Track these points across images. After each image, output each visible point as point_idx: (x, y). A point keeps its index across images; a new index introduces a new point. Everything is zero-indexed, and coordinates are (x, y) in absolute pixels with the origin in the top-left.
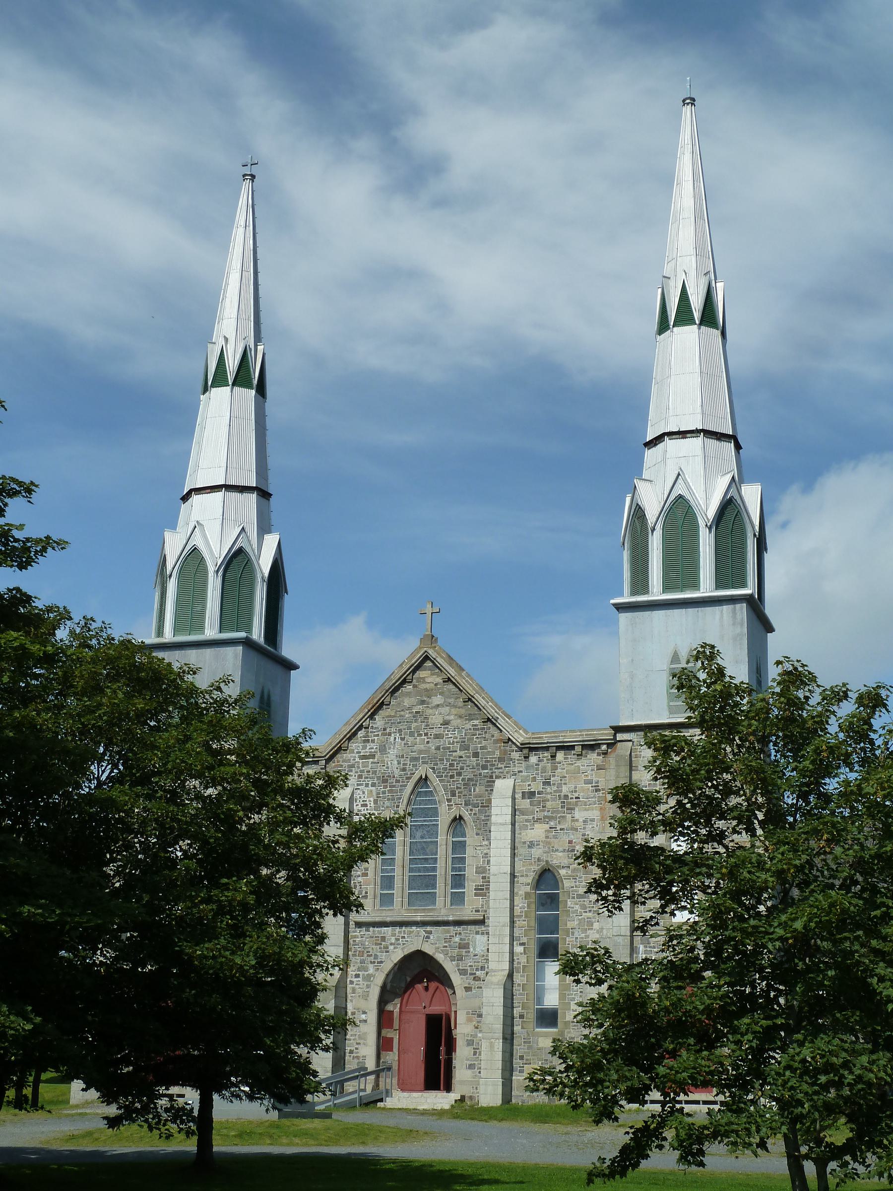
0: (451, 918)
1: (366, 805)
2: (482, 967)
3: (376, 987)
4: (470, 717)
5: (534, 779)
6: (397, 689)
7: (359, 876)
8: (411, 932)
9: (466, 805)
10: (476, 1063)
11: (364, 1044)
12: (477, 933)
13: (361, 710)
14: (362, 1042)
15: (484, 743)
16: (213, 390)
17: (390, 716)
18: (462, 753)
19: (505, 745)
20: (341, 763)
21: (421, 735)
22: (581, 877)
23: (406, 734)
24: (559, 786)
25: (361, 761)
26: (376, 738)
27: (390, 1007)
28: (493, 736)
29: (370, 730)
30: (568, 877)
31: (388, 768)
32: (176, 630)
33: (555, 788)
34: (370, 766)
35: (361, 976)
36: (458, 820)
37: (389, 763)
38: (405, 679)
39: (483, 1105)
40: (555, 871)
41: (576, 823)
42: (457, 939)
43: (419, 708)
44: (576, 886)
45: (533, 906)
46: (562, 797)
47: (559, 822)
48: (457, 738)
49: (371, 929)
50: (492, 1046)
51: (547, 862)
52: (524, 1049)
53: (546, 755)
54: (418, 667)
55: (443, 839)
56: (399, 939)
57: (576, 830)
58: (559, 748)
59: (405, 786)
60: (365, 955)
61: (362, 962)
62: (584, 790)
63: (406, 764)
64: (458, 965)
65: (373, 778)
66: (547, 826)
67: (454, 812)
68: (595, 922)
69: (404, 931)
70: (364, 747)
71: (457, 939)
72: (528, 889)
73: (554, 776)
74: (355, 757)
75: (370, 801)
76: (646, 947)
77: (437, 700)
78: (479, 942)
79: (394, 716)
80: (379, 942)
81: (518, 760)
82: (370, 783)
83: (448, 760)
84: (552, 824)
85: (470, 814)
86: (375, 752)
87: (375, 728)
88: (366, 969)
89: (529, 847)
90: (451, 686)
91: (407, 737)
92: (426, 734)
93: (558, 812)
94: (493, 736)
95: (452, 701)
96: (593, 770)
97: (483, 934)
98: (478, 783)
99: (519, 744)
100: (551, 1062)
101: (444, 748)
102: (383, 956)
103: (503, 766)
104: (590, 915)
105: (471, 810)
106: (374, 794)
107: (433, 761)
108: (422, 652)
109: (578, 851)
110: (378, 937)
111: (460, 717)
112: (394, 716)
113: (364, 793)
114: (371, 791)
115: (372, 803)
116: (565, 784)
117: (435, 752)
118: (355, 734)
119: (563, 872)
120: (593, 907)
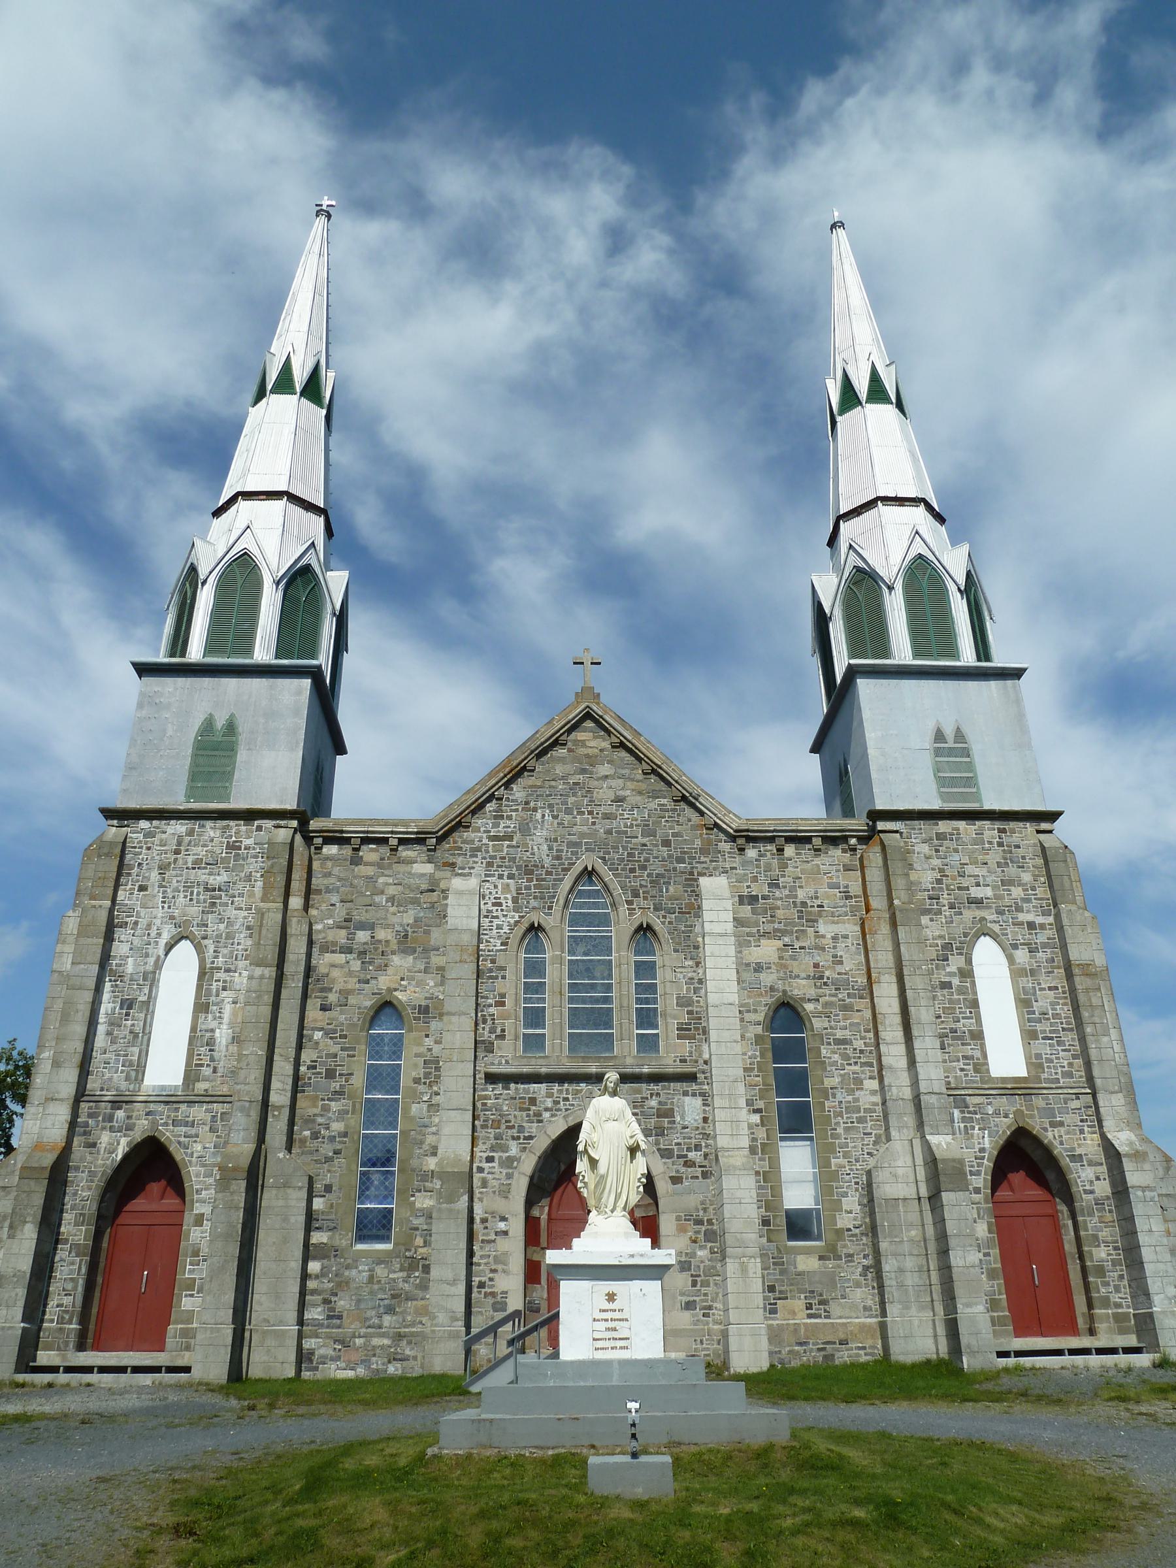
0: (646, 1070)
1: (500, 904)
2: (696, 1146)
3: (522, 1176)
4: (655, 795)
5: (755, 880)
6: (544, 752)
7: (491, 1006)
8: (578, 1092)
9: (656, 909)
10: (697, 1299)
11: (504, 1271)
12: (685, 1094)
13: (490, 775)
14: (499, 1267)
15: (677, 829)
16: (274, 396)
17: (535, 786)
18: (645, 840)
19: (708, 832)
20: (459, 844)
21: (583, 813)
22: (837, 1015)
23: (559, 810)
24: (793, 889)
25: (491, 843)
26: (514, 814)
27: (535, 1212)
28: (690, 820)
29: (504, 802)
30: (819, 1015)
31: (533, 854)
32: (209, 649)
33: (787, 892)
34: (505, 850)
35: (496, 1160)
36: (645, 931)
37: (535, 847)
38: (557, 740)
39: (738, 1370)
40: (796, 1005)
41: (822, 940)
42: (653, 1103)
43: (580, 778)
44: (831, 1028)
45: (770, 1055)
46: (799, 905)
47: (797, 938)
48: (636, 820)
49: (512, 1086)
50: (744, 1269)
51: (784, 992)
52: (774, 1274)
53: (769, 848)
54: (575, 727)
55: (623, 958)
56: (558, 1103)
57: (823, 949)
58: (789, 840)
59: (562, 880)
60: (503, 1127)
61: (498, 1137)
62: (829, 897)
63: (562, 851)
64: (657, 1143)
65: (510, 867)
66: (780, 944)
67: (638, 918)
68: (865, 1079)
69: (567, 1090)
70: (496, 825)
71: (653, 1103)
72: (759, 1029)
73: (783, 876)
74: (482, 837)
75: (506, 898)
76: (962, 1112)
77: (605, 769)
78: (690, 1109)
79: (540, 787)
80: (526, 1106)
81: (729, 853)
82: (506, 873)
83: (625, 848)
84: (787, 940)
85: (663, 923)
86: (512, 832)
87: (513, 801)
88: (505, 1149)
89: (756, 971)
90: (624, 754)
91: (561, 815)
92: (590, 813)
93: (794, 924)
94: (690, 820)
95: (626, 772)
96: (839, 870)
97: (694, 1095)
98: (672, 881)
99: (731, 831)
100: (821, 1295)
101: (618, 832)
102: (533, 1128)
103: (707, 860)
104: (857, 1068)
105: (665, 917)
106: (513, 888)
107: (602, 847)
108: (583, 706)
109: (828, 978)
110: (524, 1098)
111: (640, 793)
112: (540, 787)
113: (496, 887)
114: (508, 885)
115: (510, 902)
116: (801, 887)
117: (604, 836)
118: (481, 806)
119: (809, 1007)
120: (860, 1058)
